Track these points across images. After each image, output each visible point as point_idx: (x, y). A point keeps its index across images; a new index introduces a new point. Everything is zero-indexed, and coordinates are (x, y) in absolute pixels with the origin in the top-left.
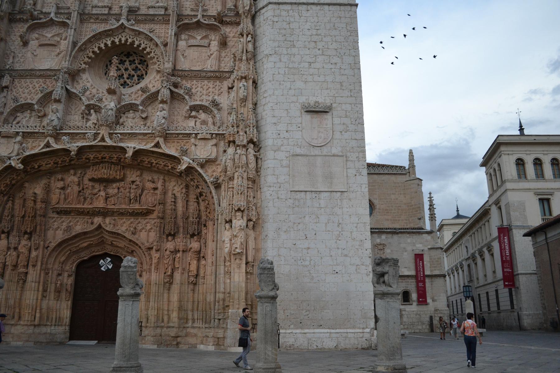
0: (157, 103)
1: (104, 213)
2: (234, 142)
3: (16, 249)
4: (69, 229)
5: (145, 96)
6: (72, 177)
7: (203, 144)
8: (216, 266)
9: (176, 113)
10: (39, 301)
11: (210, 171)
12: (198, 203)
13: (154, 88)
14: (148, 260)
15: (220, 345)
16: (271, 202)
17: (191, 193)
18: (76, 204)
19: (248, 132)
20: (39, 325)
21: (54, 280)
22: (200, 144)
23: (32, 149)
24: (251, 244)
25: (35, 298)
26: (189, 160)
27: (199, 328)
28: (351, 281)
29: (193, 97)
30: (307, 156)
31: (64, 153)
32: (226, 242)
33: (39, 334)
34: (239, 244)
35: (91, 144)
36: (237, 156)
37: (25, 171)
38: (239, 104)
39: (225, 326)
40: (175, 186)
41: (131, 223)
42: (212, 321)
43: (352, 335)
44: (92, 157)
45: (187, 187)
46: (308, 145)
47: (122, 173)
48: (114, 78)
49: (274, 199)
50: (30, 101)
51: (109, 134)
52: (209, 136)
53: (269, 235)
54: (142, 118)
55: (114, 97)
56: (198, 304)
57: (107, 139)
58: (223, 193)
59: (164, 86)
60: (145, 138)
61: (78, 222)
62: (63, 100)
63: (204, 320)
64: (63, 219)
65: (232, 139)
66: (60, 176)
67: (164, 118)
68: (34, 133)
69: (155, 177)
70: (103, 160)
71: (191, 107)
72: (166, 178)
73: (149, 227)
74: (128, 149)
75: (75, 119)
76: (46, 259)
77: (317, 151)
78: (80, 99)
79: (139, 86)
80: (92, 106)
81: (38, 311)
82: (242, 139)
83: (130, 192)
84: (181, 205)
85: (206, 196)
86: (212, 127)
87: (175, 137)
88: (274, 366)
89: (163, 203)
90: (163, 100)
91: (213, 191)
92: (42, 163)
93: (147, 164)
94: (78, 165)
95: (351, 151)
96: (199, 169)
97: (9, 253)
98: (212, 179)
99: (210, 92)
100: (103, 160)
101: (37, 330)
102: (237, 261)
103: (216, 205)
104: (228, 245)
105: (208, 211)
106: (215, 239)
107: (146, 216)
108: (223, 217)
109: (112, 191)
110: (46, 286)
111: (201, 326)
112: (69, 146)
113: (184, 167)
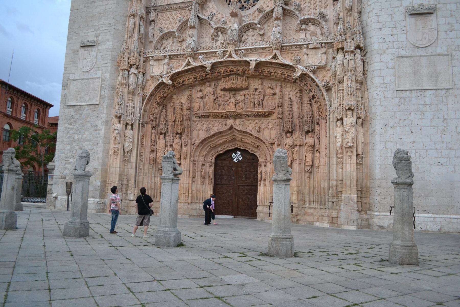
0: (271, 20)
1: (235, 116)
2: (342, 49)
3: (171, 146)
4: (208, 129)
5: (261, 15)
6: (208, 88)
7: (314, 53)
8: (330, 157)
9: (288, 28)
10: (190, 185)
11: (321, 76)
12: (311, 105)
13: (268, 8)
14: (271, 153)
15: (334, 223)
16: (378, 101)
17: (305, 96)
18: (212, 110)
19: (355, 39)
20: (191, 203)
21: (200, 169)
22: (311, 53)
23: (177, 68)
24: (361, 139)
25: (187, 182)
26: (302, 68)
27: (315, 208)
28: (455, 172)
29: (302, 12)
30: (412, 57)
31: (200, 70)
32: (338, 137)
33: (192, 209)
34: (350, 138)
35: (221, 60)
36: (346, 62)
37: (173, 86)
38: (345, 13)
39: (338, 207)
40: (290, 91)
41: (256, 123)
42: (327, 203)
43: (455, 221)
44: (222, 70)
45: (301, 91)
46: (413, 46)
47: (247, 83)
48: (235, 3)
49: (380, 98)
50: (171, 30)
51: (235, 50)
52: (319, 46)
53: (376, 131)
54: (260, 35)
55: (237, 19)
56: (313, 189)
57: (234, 55)
58: (333, 95)
59: (277, 4)
60: (264, 51)
61: (215, 124)
62: (196, 26)
63: (319, 202)
64: (203, 122)
65: (340, 46)
66: (198, 88)
67: (279, 33)
68: (177, 55)
69: (274, 84)
70: (232, 73)
71: (301, 21)
72: (283, 85)
73: (270, 126)
74: (251, 62)
75: (207, 41)
76: (193, 153)
77: (422, 52)
78: (209, 24)
79: (255, 8)
80: (219, 29)
81: (190, 192)
82: (350, 45)
83: (254, 98)
84: (296, 107)
85: (318, 98)
86: (321, 37)
87: (290, 48)
88: (411, 245)
89: (281, 106)
90: (277, 17)
91: (325, 94)
92: (185, 78)
93: (267, 74)
94: (212, 78)
95: (457, 49)
96: (312, 75)
97: (166, 149)
98: (323, 83)
99: (316, 6)
100: (232, 73)
101: (190, 206)
102: (349, 153)
103: (328, 105)
104: (340, 140)
105: (321, 111)
106: (328, 135)
107: (268, 117)
108: (335, 116)
109: (240, 97)
110: (194, 174)
111: (316, 207)
112: (204, 63)
113: (298, 74)
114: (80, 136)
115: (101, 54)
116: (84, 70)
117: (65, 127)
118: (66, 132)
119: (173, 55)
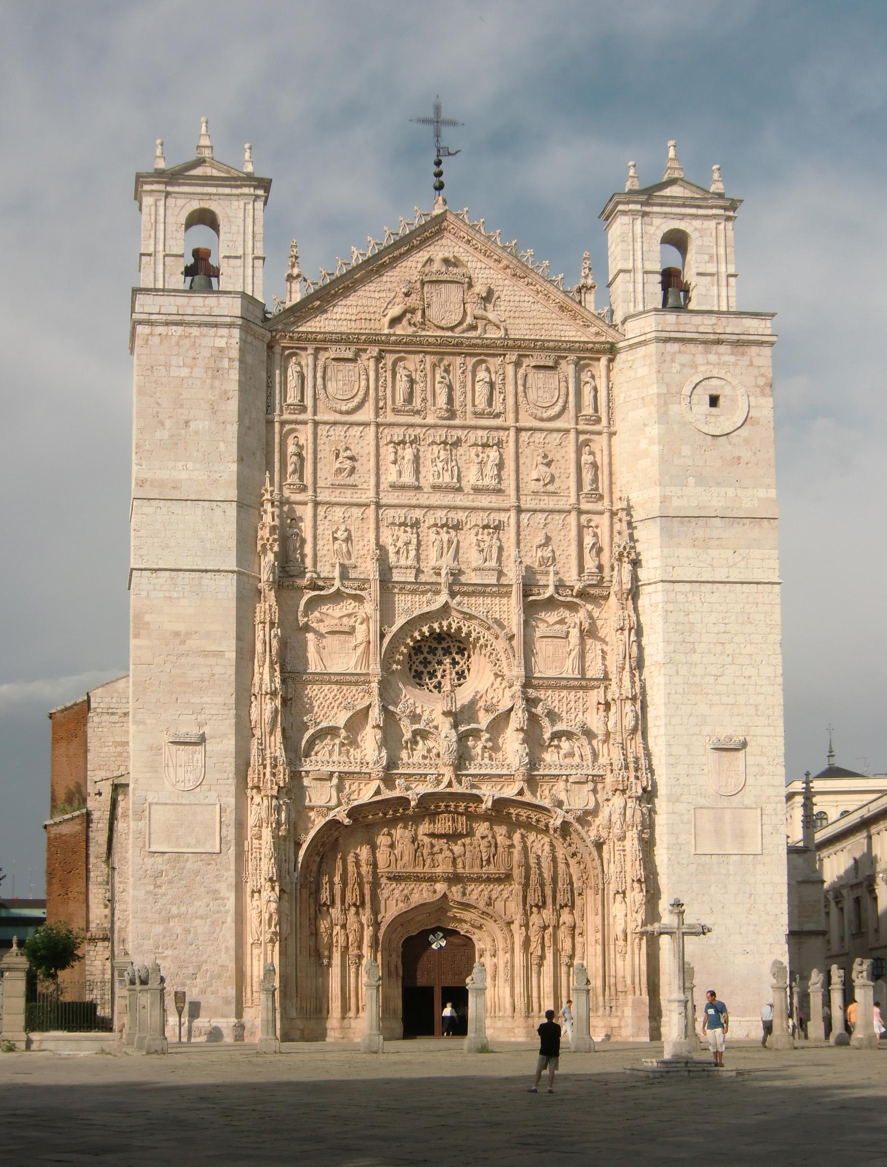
35: (436, 790)
68: (354, 773)
74: (485, 799)
114: (183, 909)
115: (215, 760)
116: (181, 786)
117: (148, 892)
118: (151, 900)
119: (346, 773)
